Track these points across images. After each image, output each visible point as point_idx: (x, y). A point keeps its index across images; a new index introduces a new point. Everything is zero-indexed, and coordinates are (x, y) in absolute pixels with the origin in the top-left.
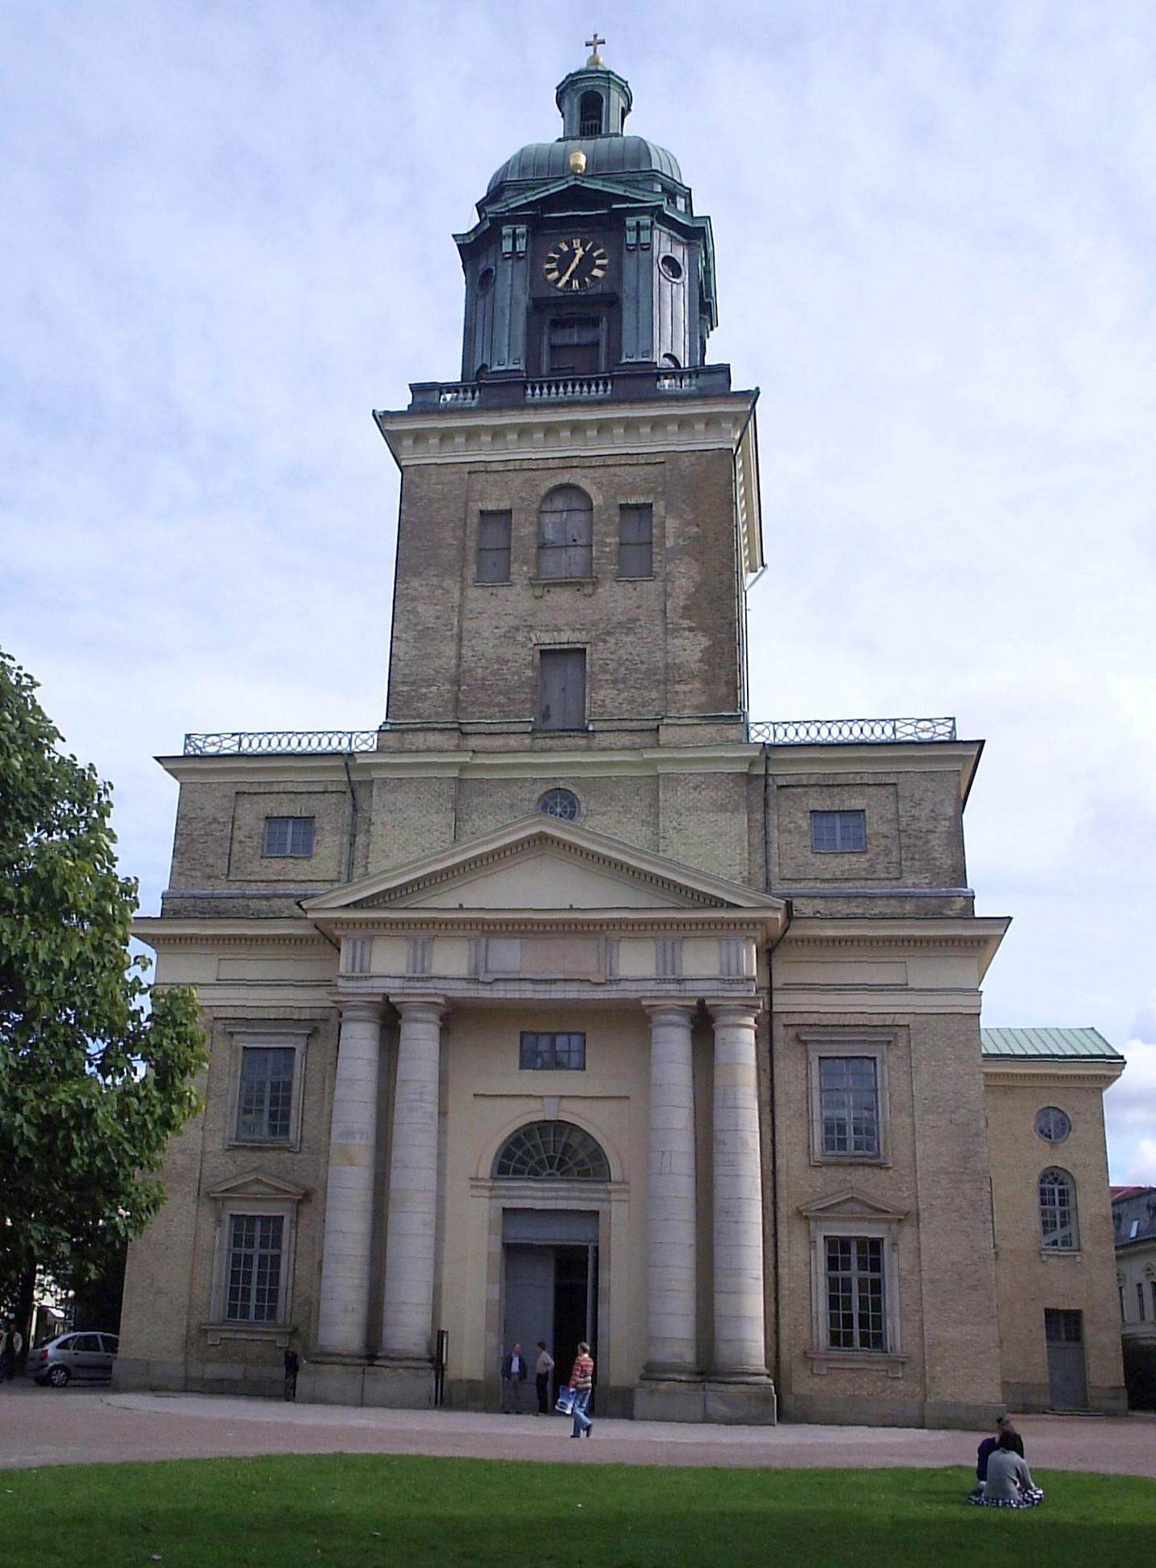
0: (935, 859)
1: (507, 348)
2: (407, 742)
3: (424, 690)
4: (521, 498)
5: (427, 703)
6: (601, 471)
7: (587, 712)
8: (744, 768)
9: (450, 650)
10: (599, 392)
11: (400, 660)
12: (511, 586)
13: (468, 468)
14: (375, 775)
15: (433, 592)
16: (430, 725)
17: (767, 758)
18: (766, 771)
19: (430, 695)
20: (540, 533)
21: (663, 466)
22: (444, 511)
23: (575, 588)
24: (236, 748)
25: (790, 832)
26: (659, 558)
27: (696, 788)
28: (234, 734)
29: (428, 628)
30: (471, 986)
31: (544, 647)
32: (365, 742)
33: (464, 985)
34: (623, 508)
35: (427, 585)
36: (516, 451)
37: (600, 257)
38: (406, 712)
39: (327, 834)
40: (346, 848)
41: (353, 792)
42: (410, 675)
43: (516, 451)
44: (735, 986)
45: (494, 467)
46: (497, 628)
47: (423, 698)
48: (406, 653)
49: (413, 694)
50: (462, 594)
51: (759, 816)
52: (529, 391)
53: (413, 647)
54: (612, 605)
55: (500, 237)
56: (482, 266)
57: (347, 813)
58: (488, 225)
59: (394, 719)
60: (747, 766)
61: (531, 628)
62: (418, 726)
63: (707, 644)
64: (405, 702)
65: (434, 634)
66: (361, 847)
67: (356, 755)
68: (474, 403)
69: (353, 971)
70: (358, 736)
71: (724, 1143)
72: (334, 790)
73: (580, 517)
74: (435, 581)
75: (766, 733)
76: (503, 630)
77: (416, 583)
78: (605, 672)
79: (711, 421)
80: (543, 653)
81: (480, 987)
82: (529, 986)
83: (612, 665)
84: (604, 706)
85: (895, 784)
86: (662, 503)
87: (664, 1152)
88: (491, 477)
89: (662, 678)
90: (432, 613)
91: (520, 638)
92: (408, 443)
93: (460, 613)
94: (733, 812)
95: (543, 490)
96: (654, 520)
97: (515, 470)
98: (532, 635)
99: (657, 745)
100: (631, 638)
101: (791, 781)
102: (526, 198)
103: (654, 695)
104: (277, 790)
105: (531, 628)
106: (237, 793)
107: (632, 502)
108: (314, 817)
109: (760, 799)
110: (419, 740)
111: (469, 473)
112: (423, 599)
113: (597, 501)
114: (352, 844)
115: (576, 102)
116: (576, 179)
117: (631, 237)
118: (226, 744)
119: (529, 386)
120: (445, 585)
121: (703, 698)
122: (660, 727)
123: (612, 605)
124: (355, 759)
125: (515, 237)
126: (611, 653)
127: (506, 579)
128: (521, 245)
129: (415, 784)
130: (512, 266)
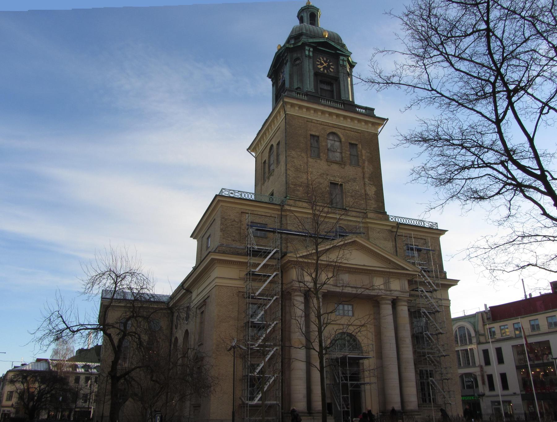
0: (436, 262)
1: (308, 85)
3: (298, 188)
4: (322, 133)
5: (299, 193)
6: (343, 131)
7: (344, 204)
8: (390, 228)
9: (305, 177)
10: (339, 106)
12: (321, 160)
13: (306, 120)
16: (301, 200)
17: (398, 227)
18: (397, 231)
20: (327, 145)
21: (359, 134)
22: (300, 131)
23: (339, 165)
24: (240, 196)
25: (401, 249)
26: (361, 161)
27: (378, 232)
28: (239, 191)
30: (334, 287)
31: (331, 181)
33: (332, 287)
34: (351, 144)
36: (319, 118)
37: (332, 65)
43: (319, 118)
44: (404, 294)
45: (314, 121)
46: (318, 172)
47: (298, 191)
50: (308, 160)
51: (394, 243)
52: (321, 101)
54: (349, 173)
55: (304, 50)
56: (295, 56)
58: (300, 44)
60: (391, 228)
61: (327, 175)
62: (298, 199)
63: (376, 190)
67: (285, 206)
68: (306, 99)
71: (405, 341)
73: (337, 144)
74: (299, 153)
75: (393, 219)
76: (319, 173)
77: (293, 152)
78: (349, 192)
79: (366, 122)
80: (331, 183)
81: (337, 288)
82: (350, 289)
83: (351, 191)
84: (349, 203)
85: (425, 239)
86: (360, 145)
87: (391, 343)
88: (313, 124)
89: (364, 197)
91: (324, 177)
92: (289, 106)
93: (307, 165)
94: (388, 241)
95: (328, 133)
96: (359, 150)
97: (320, 124)
98: (328, 177)
99: (367, 217)
100: (355, 184)
101: (401, 234)
102: (313, 40)
103: (362, 202)
105: (327, 175)
106: (242, 212)
107: (353, 142)
108: (267, 225)
109: (393, 238)
110: (300, 204)
111: (307, 121)
113: (343, 140)
115: (309, 14)
116: (327, 40)
117: (341, 62)
118: (237, 194)
119: (321, 99)
120: (302, 155)
121: (376, 206)
122: (368, 213)
123: (349, 173)
125: (309, 51)
126: (350, 187)
127: (319, 157)
128: (311, 54)
130: (309, 60)
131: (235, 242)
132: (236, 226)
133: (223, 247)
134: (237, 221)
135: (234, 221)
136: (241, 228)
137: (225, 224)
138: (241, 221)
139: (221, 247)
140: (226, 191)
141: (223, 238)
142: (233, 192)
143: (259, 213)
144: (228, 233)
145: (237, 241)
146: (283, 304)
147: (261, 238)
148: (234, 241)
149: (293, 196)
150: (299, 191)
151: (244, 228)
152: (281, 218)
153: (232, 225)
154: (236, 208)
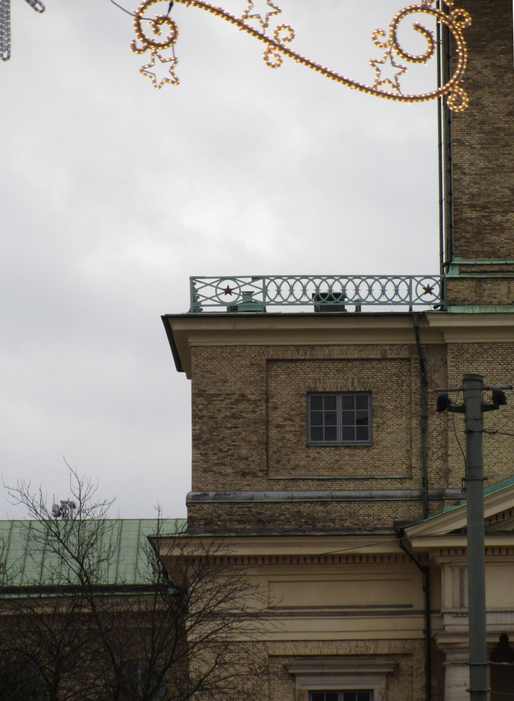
2: (486, 293)
3: (498, 218)
5: (503, 237)
11: (464, 173)
14: (449, 339)
15: (502, 77)
19: (508, 225)
28: (255, 278)
29: (498, 129)
32: (428, 290)
35: (492, 65)
38: (476, 247)
39: (390, 415)
40: (417, 434)
41: (422, 362)
42: (479, 195)
48: (472, 164)
49: (486, 223)
53: (481, 155)
57: (414, 387)
59: (464, 256)
64: (474, 233)
65: (507, 138)
66: (435, 434)
67: (429, 317)
69: (462, 606)
70: (419, 282)
72: (394, 356)
90: (502, 107)
104: (322, 357)
106: (269, 361)
108: (370, 392)
112: (490, 86)
114: (424, 430)
124: (428, 322)
129: (501, 351)
131: (249, 477)
132: (249, 416)
133: (206, 506)
134: (253, 397)
135: (243, 395)
136: (268, 422)
137: (210, 417)
138: (267, 397)
139: (198, 507)
140: (207, 285)
141: (205, 471)
142: (232, 284)
143: (337, 354)
144: (221, 450)
145: (254, 475)
146: (434, 683)
147: (347, 451)
148: (244, 474)
149: (477, 254)
150: (503, 230)
151: (279, 421)
152: (422, 362)
153: (234, 416)
154: (245, 346)
